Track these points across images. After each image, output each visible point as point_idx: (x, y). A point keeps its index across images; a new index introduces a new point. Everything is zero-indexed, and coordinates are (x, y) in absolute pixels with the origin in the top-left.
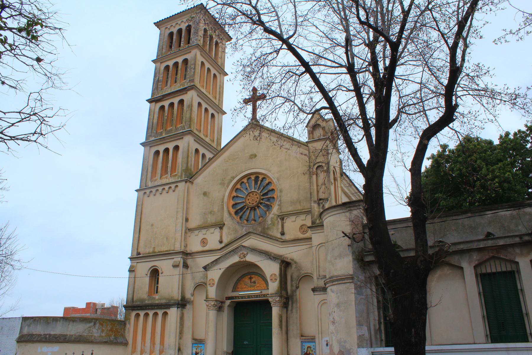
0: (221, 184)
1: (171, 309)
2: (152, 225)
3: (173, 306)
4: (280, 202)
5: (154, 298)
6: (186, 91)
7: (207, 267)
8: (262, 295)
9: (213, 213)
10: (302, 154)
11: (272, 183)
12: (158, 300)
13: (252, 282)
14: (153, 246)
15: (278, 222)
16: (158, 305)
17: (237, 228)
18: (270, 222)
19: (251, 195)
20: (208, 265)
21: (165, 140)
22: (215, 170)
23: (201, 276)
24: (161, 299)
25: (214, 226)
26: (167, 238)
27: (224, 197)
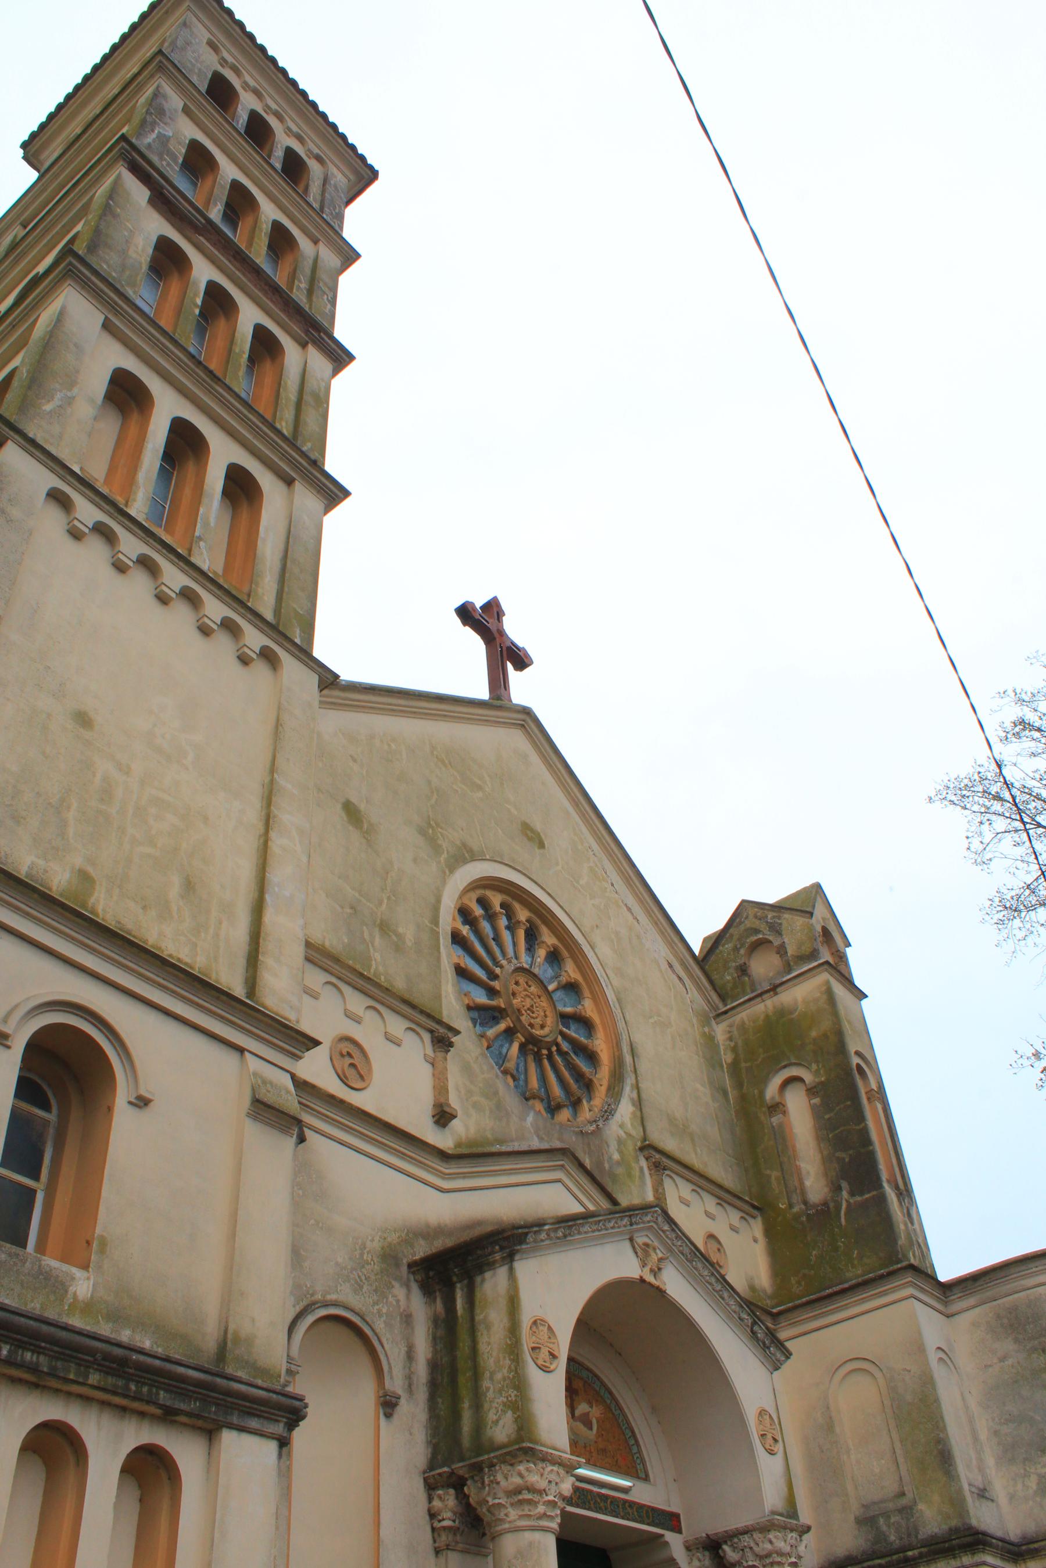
0: (422, 832)
1: (228, 1438)
2: (83, 719)
3: (254, 1423)
4: (635, 1095)
5: (58, 1287)
6: (307, 332)
7: (530, 1238)
8: (632, 1504)
9: (394, 938)
10: (671, 966)
11: (586, 992)
12: (88, 1308)
13: (577, 1413)
14: (78, 861)
15: (641, 1169)
16: (123, 1362)
17: (501, 1094)
18: (616, 1156)
19: (522, 981)
20: (540, 1224)
21: (210, 392)
22: (393, 746)
23: (340, 1260)
24: (115, 1316)
25: (409, 1011)
26: (189, 886)
27: (438, 901)
